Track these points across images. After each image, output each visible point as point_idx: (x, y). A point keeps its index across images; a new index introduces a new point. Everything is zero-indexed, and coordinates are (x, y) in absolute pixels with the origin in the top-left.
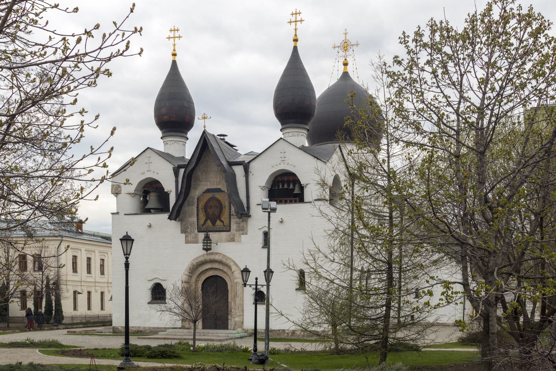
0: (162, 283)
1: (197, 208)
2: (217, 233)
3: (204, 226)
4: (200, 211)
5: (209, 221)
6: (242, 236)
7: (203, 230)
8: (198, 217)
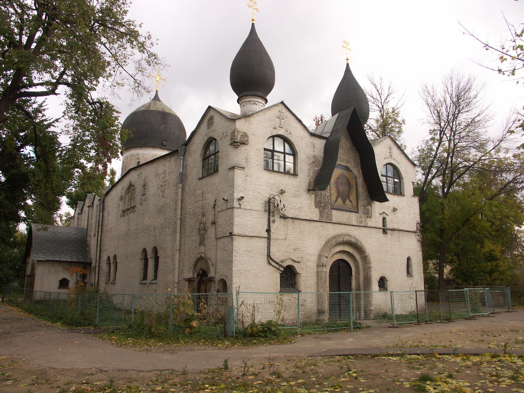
0: (295, 265)
2: (348, 213)
5: (340, 199)
7: (335, 207)
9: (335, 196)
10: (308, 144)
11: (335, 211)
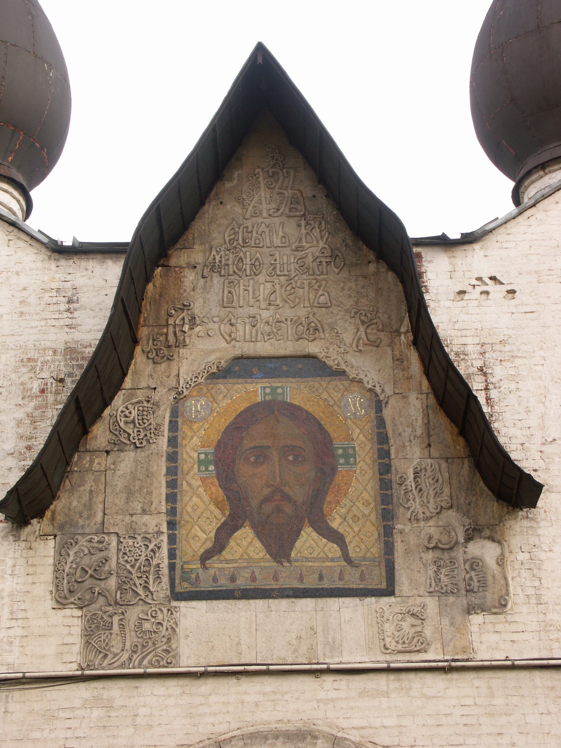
1: (172, 458)
2: (308, 603)
3: (215, 564)
6: (477, 619)
7: (206, 585)
8: (172, 512)
9: (215, 525)
10: (33, 299)
11: (201, 605)
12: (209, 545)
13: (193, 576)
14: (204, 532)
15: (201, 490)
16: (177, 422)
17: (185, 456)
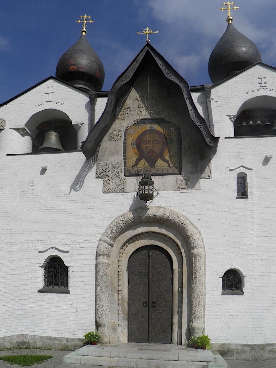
1: (125, 143)
3: (136, 168)
4: (130, 148)
8: (125, 156)
12: (134, 164)
13: (130, 171)
14: (133, 161)
15: (132, 150)
16: (126, 135)
17: (128, 143)
